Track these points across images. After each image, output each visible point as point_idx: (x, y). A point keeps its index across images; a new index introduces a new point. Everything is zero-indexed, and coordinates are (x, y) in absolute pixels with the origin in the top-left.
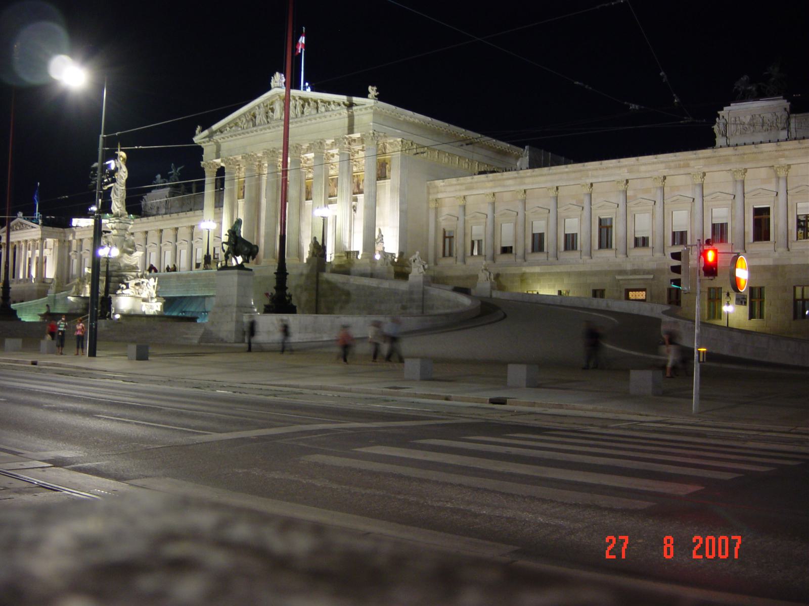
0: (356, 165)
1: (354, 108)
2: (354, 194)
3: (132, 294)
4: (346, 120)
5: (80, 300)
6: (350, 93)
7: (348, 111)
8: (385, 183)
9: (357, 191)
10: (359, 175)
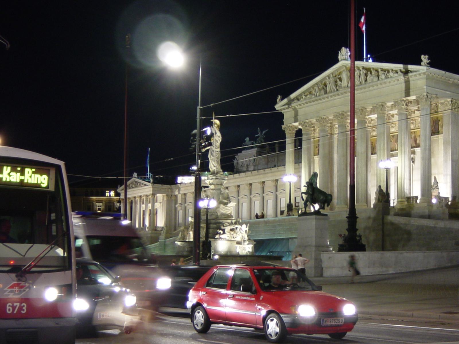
0: (413, 123)
1: (410, 74)
2: (412, 148)
3: (227, 238)
4: (403, 85)
5: (186, 244)
6: (405, 62)
7: (405, 78)
8: (438, 137)
9: (415, 145)
10: (416, 132)
